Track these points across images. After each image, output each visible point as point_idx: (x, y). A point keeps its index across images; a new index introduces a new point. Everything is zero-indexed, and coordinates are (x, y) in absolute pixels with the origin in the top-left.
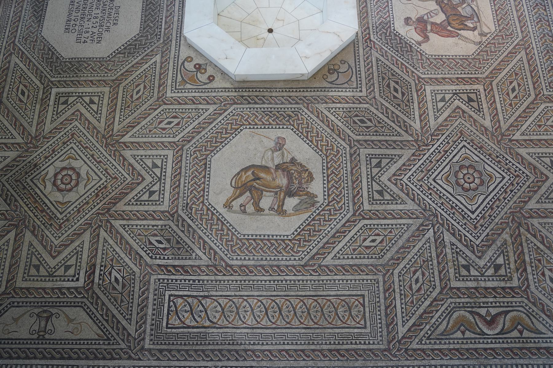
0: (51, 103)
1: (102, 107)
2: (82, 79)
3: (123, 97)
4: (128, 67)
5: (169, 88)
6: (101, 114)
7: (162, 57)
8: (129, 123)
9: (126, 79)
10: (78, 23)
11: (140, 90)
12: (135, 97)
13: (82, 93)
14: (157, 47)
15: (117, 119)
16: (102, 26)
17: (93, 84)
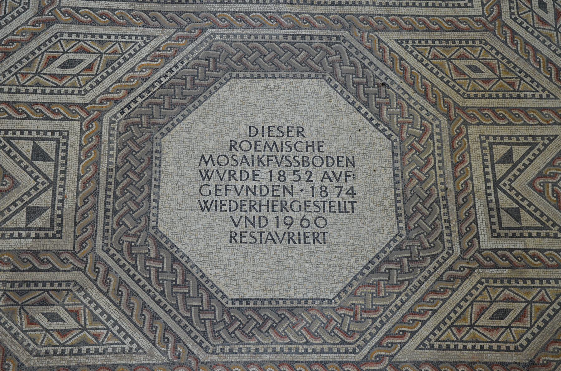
0: (520, 244)
1: (517, 137)
2: (450, 186)
3: (490, 97)
4: (415, 96)
5: (461, 12)
6: (534, 137)
7: (386, 29)
8: (550, 79)
9: (445, 95)
10: (297, 216)
11: (470, 67)
12: (487, 73)
13: (487, 181)
14: (361, 41)
15: (543, 103)
16: (305, 160)
17: (462, 162)
